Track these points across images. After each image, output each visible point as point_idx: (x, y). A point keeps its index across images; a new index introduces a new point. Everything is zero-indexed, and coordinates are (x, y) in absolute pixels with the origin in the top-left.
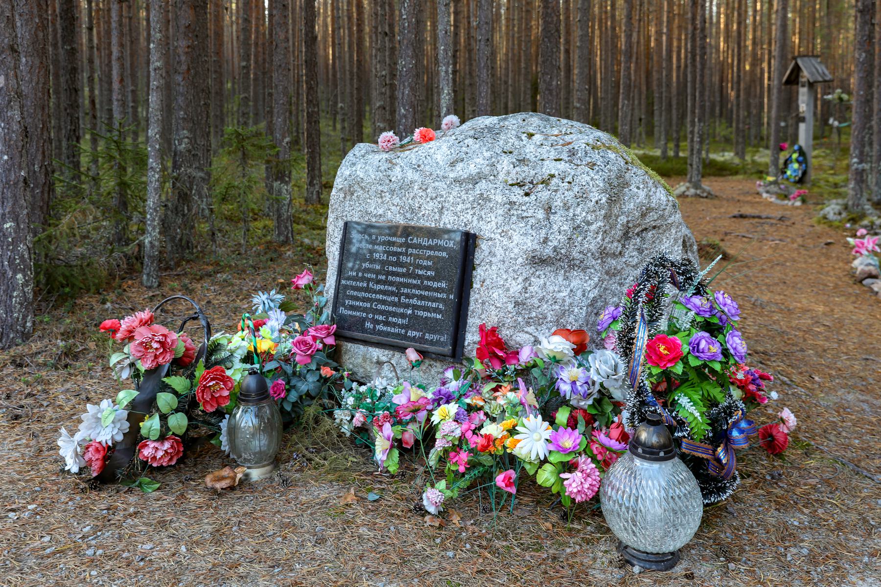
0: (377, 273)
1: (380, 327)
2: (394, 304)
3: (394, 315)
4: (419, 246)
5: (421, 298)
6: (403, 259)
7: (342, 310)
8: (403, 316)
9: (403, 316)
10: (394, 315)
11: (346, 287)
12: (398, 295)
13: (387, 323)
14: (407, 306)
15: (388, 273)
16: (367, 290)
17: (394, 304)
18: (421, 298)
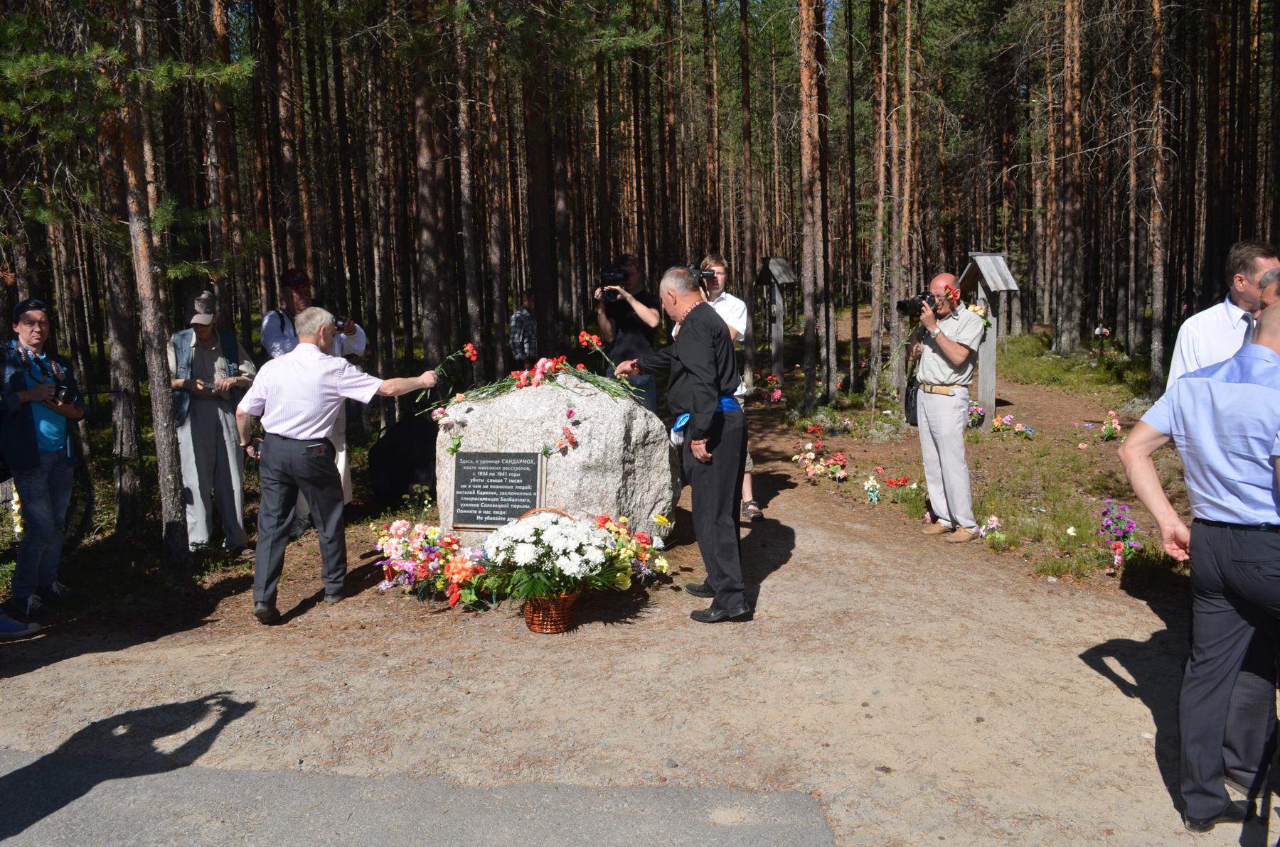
0: (482, 484)
1: (488, 518)
2: (496, 503)
3: (497, 509)
4: (510, 465)
5: (515, 497)
6: (500, 474)
7: (459, 511)
8: (503, 509)
9: (503, 509)
10: (497, 509)
11: (460, 496)
12: (499, 497)
13: (492, 515)
14: (504, 503)
15: (490, 484)
16: (476, 496)
17: (496, 503)
18: (515, 497)
